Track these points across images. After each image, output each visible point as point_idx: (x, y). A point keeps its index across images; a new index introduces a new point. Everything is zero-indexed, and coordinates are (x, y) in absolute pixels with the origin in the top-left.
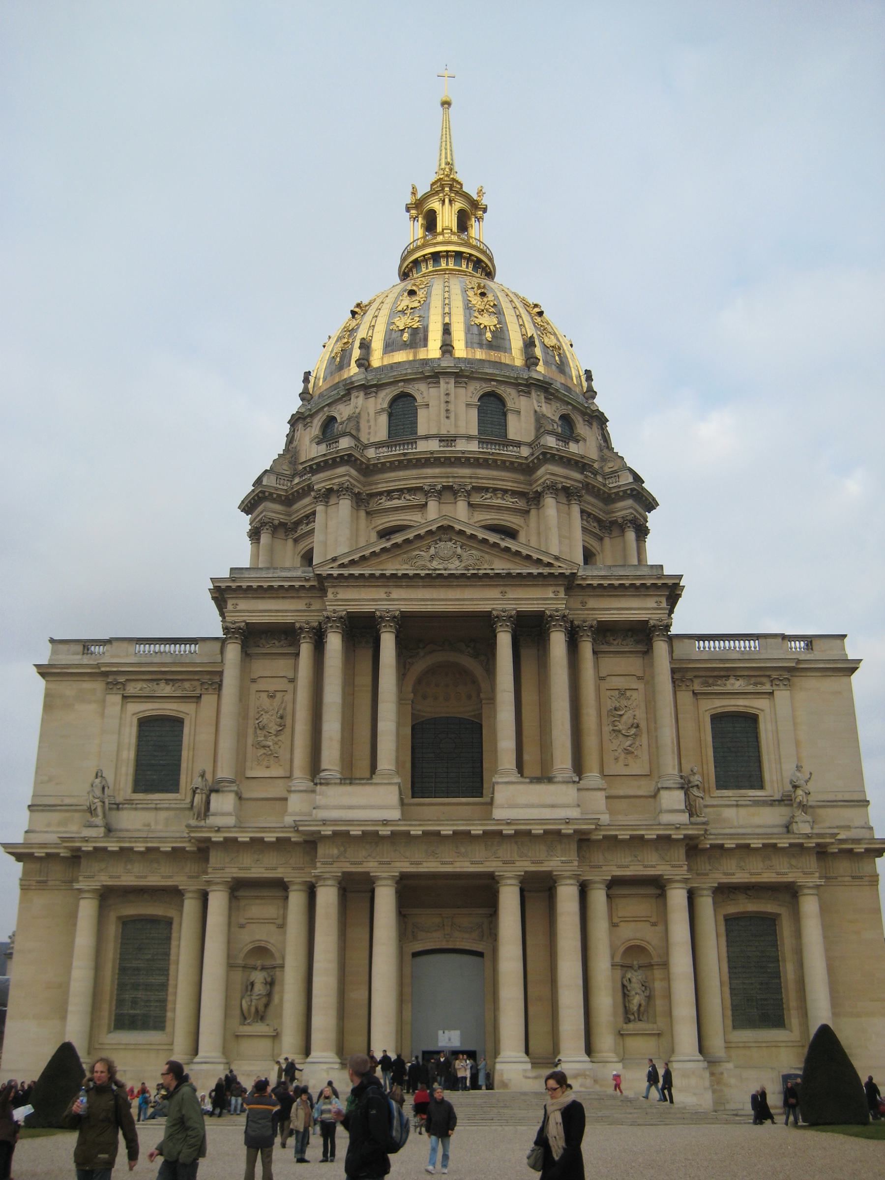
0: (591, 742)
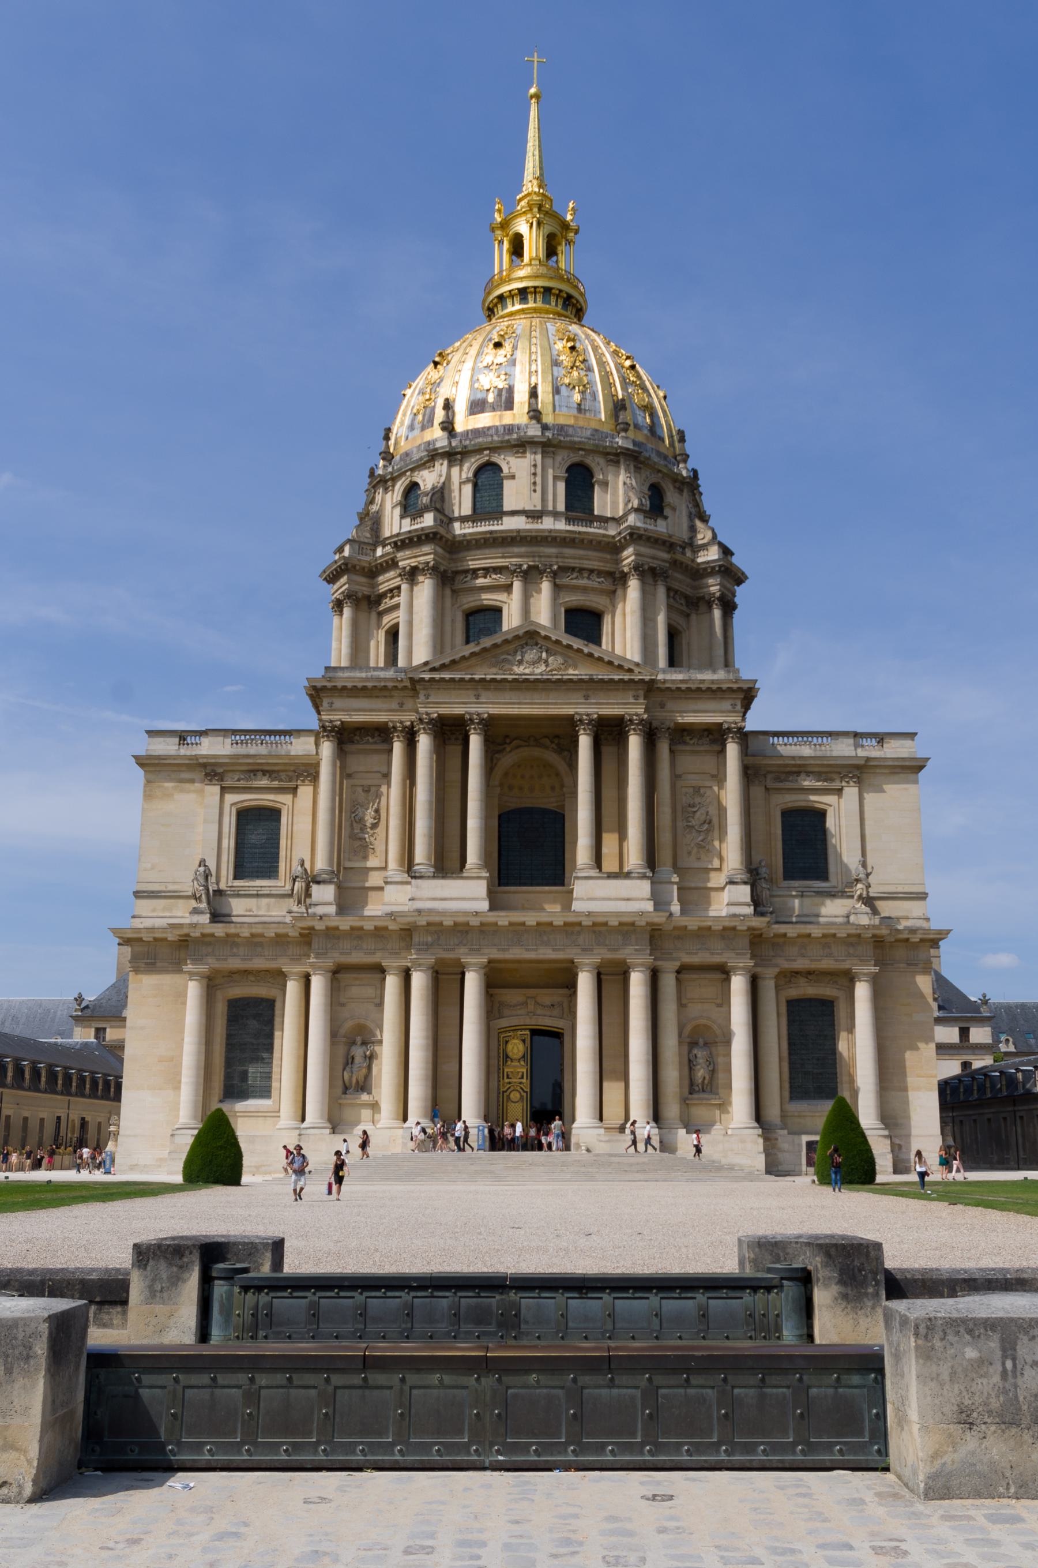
0: (664, 838)
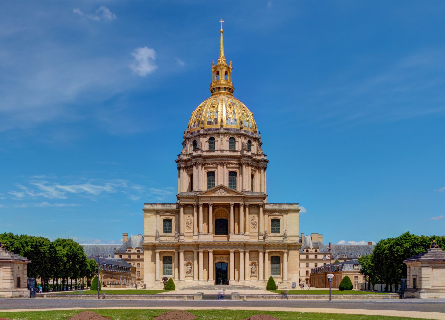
0: (247, 227)
